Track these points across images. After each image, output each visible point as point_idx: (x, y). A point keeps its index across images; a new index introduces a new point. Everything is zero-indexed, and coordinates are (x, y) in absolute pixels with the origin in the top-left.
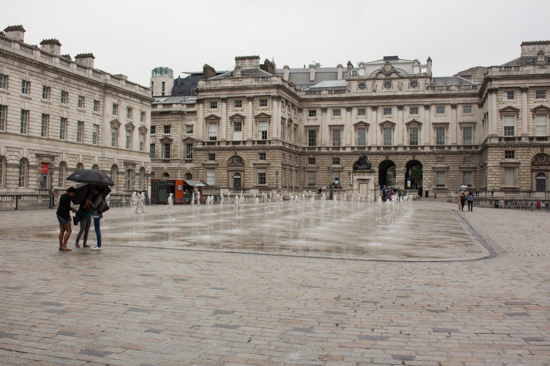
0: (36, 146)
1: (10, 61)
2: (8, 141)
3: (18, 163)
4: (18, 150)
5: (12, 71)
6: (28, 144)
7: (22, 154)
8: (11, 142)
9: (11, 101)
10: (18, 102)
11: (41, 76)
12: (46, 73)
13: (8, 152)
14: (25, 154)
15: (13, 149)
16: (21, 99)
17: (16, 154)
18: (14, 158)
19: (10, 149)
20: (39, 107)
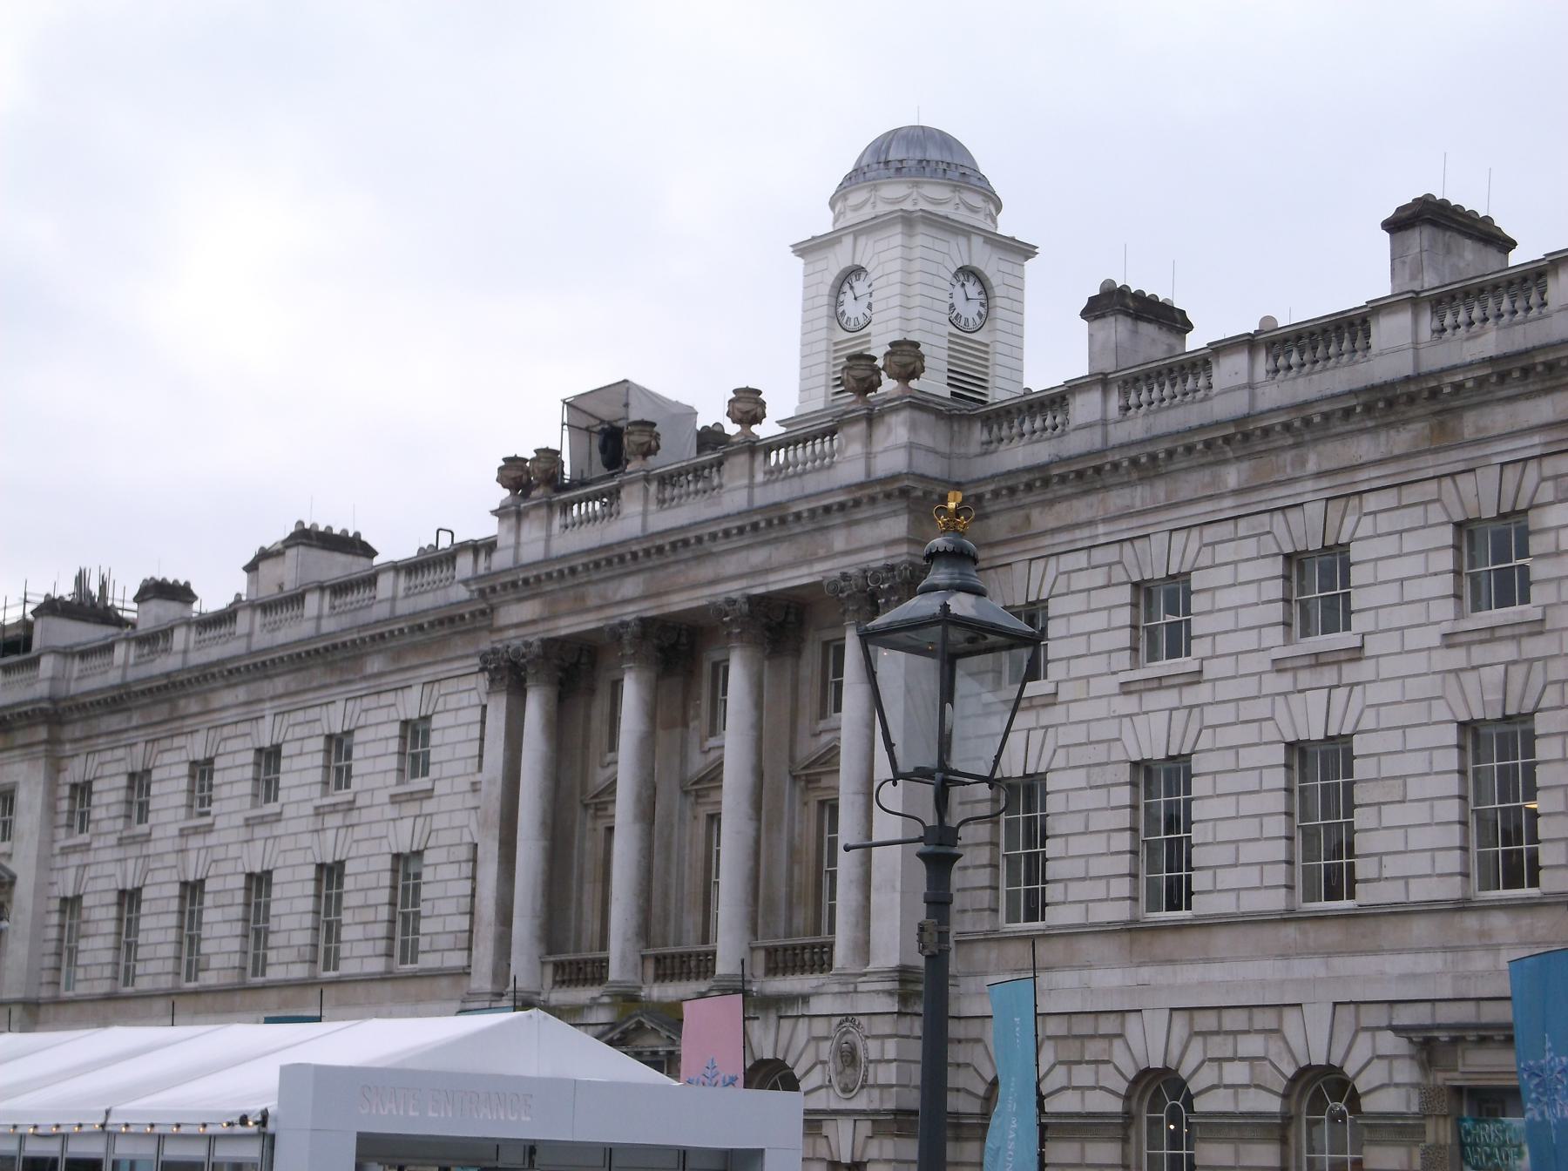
0: (1415, 971)
1: (1191, 484)
2: (1191, 974)
3: (1274, 1105)
4: (1265, 1020)
5: (1210, 534)
6: (1346, 965)
7: (1296, 1042)
8: (1216, 972)
9: (1212, 715)
10: (1261, 709)
11: (1430, 465)
12: (1470, 424)
13: (1197, 1043)
14: (1312, 1040)
15: (1232, 1021)
16: (1284, 682)
17: (1251, 1045)
18: (1237, 1073)
19: (1207, 1022)
20: (1428, 686)
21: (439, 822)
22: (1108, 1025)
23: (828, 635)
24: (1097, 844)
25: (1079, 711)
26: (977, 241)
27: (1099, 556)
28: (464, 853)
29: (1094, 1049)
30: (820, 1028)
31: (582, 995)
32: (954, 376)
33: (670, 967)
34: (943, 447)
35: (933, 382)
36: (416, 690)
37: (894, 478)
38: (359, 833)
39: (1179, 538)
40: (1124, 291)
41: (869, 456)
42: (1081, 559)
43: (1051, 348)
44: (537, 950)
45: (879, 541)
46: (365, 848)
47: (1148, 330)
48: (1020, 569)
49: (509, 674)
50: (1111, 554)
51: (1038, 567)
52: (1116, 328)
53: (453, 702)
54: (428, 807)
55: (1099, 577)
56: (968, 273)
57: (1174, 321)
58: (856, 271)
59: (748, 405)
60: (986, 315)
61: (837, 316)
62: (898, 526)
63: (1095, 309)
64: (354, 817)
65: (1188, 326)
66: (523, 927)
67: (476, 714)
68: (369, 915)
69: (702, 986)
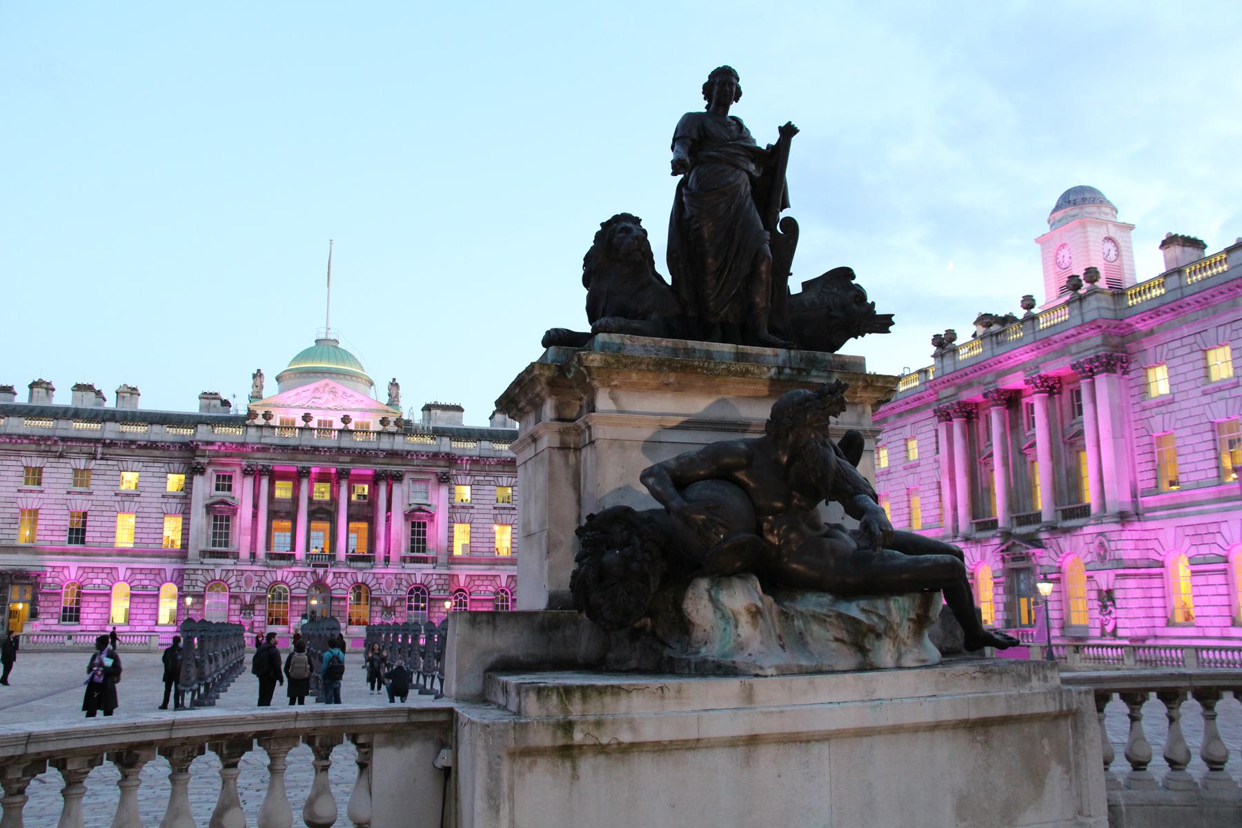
21: (923, 475)
22: (1213, 528)
23: (1072, 387)
24: (1200, 457)
25: (1184, 405)
26: (1110, 226)
27: (1185, 341)
28: (935, 486)
29: (1207, 539)
30: (1088, 539)
31: (989, 533)
32: (1109, 280)
33: (1023, 520)
34: (1112, 307)
35: (1102, 284)
36: (908, 427)
37: (1095, 321)
38: (893, 482)
39: (1221, 329)
40: (1176, 236)
41: (1082, 314)
42: (1178, 343)
43: (1147, 264)
44: (969, 519)
45: (1092, 345)
46: (896, 487)
47: (1189, 250)
48: (1151, 351)
49: (945, 416)
50: (1191, 340)
51: (1159, 349)
52: (1176, 250)
53: (923, 429)
54: (918, 469)
55: (1187, 350)
56: (1109, 239)
57: (1197, 244)
58: (1063, 246)
59: (1028, 302)
60: (1118, 254)
61: (1058, 264)
62: (1098, 340)
63: (1165, 244)
64: (890, 476)
65: (1204, 246)
66: (962, 511)
67: (933, 433)
68: (900, 512)
69: (1037, 527)
